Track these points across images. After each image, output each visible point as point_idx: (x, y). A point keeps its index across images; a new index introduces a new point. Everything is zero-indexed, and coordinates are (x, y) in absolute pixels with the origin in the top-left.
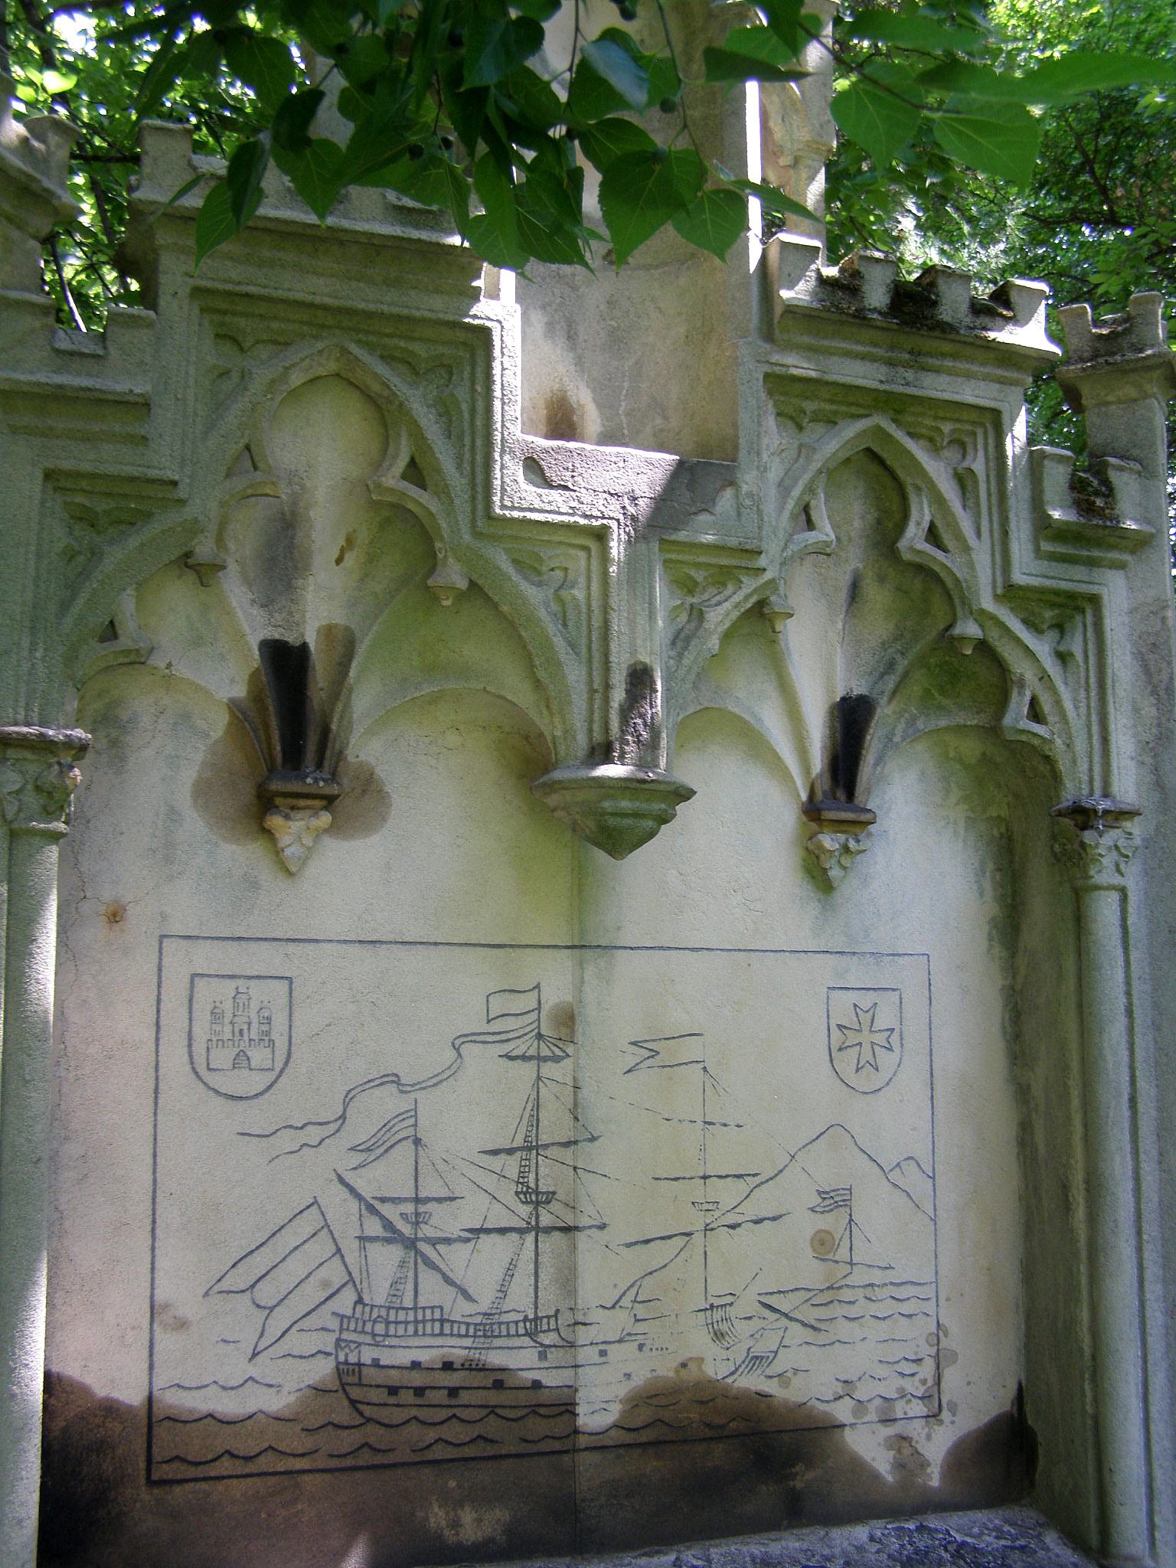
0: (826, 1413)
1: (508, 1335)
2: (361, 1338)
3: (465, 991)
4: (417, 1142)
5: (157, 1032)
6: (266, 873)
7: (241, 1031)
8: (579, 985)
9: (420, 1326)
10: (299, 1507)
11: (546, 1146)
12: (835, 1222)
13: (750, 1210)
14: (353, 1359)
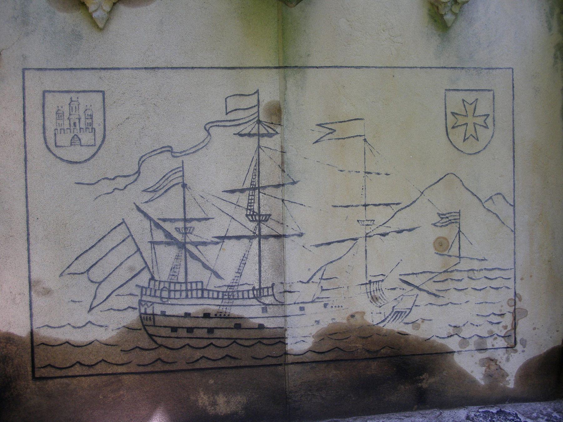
0: (442, 345)
1: (243, 298)
2: (154, 300)
3: (213, 95)
4: (184, 186)
5: (24, 126)
6: (85, 28)
7: (75, 124)
8: (284, 90)
9: (189, 293)
10: (122, 392)
11: (264, 187)
12: (449, 232)
13: (395, 225)
14: (149, 311)
